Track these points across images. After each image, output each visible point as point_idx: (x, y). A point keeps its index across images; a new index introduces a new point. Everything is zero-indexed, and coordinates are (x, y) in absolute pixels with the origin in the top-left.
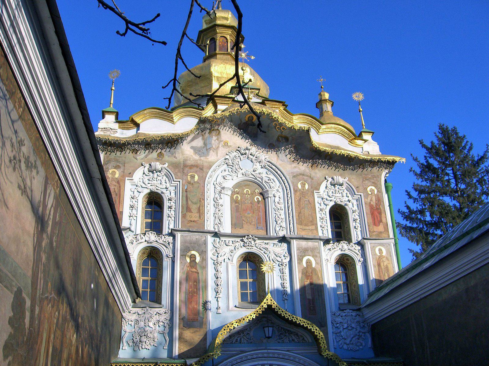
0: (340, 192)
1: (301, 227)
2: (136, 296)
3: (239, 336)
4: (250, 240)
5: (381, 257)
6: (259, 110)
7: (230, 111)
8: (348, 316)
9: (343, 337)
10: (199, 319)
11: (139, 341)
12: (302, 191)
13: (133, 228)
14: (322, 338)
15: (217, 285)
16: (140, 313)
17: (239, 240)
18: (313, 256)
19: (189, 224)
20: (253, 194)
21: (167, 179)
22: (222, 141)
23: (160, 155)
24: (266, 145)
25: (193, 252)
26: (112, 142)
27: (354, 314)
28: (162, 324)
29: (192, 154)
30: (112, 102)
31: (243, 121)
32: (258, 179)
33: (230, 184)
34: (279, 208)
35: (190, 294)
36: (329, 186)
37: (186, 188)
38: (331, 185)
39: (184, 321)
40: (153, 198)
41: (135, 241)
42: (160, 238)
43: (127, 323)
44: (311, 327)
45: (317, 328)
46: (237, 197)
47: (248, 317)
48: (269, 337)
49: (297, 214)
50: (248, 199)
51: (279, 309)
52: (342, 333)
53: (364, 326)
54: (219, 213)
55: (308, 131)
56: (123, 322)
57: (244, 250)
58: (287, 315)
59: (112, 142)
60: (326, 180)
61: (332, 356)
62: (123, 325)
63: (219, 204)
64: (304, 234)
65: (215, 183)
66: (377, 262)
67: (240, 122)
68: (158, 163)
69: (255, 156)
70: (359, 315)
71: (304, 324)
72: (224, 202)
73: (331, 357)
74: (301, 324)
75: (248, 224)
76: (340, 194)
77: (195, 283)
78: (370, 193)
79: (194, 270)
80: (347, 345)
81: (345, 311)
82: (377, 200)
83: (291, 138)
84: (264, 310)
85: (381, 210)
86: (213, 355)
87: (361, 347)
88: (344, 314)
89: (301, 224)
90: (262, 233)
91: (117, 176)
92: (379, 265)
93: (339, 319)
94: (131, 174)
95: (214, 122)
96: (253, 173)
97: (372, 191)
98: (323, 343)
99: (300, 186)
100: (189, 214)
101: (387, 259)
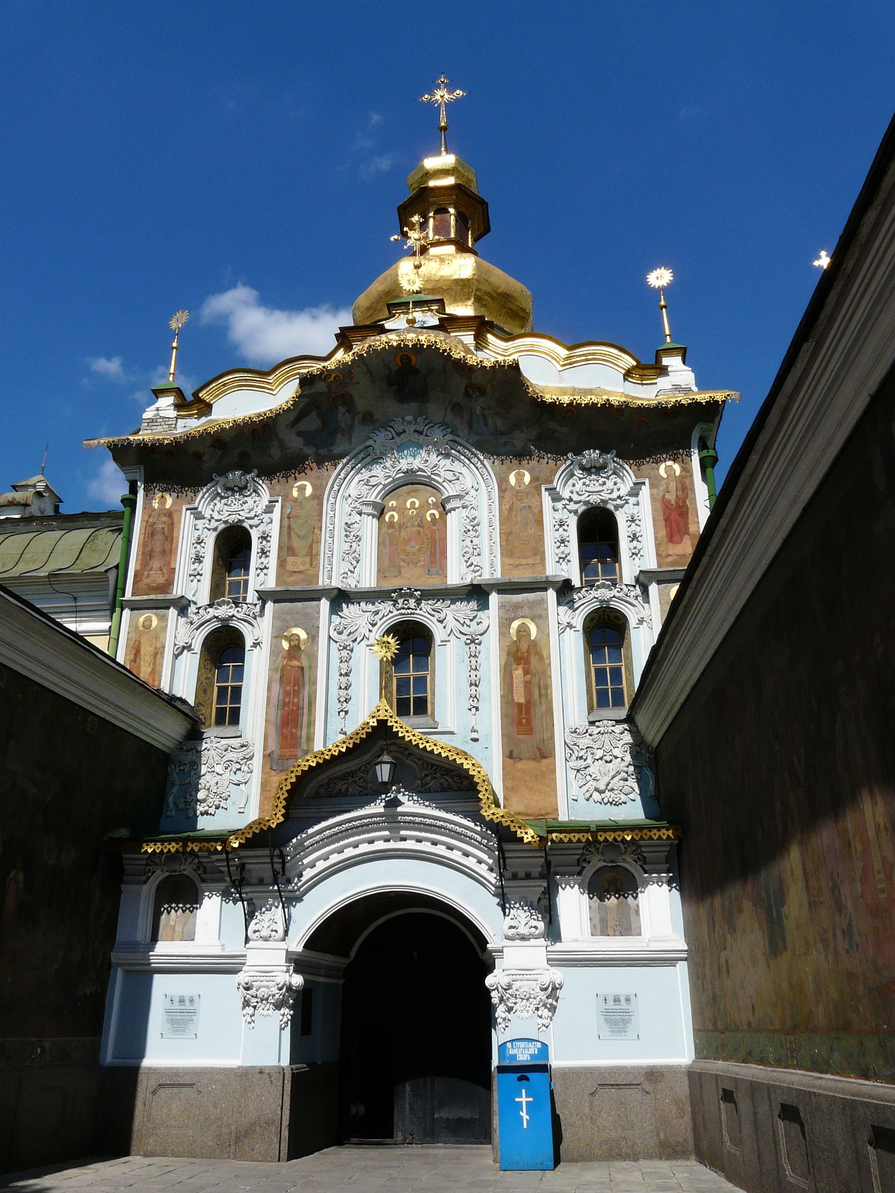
0: (600, 482)
12: (518, 488)
13: (194, 599)
14: (484, 781)
20: (425, 506)
21: (257, 499)
22: (359, 413)
23: (243, 456)
24: (447, 409)
27: (619, 728)
31: (394, 368)
34: (471, 528)
35: (286, 708)
37: (288, 511)
38: (583, 468)
42: (239, 609)
44: (463, 761)
46: (392, 516)
47: (337, 746)
49: (504, 538)
54: (351, 552)
55: (515, 368)
60: (568, 462)
61: (503, 816)
63: (352, 534)
69: (425, 433)
71: (449, 754)
74: (444, 755)
76: (600, 485)
77: (296, 688)
78: (665, 476)
79: (296, 663)
80: (601, 792)
81: (597, 724)
82: (680, 486)
86: (268, 821)
89: (512, 556)
90: (432, 583)
91: (167, 507)
95: (332, 379)
99: (512, 479)
100: (290, 559)
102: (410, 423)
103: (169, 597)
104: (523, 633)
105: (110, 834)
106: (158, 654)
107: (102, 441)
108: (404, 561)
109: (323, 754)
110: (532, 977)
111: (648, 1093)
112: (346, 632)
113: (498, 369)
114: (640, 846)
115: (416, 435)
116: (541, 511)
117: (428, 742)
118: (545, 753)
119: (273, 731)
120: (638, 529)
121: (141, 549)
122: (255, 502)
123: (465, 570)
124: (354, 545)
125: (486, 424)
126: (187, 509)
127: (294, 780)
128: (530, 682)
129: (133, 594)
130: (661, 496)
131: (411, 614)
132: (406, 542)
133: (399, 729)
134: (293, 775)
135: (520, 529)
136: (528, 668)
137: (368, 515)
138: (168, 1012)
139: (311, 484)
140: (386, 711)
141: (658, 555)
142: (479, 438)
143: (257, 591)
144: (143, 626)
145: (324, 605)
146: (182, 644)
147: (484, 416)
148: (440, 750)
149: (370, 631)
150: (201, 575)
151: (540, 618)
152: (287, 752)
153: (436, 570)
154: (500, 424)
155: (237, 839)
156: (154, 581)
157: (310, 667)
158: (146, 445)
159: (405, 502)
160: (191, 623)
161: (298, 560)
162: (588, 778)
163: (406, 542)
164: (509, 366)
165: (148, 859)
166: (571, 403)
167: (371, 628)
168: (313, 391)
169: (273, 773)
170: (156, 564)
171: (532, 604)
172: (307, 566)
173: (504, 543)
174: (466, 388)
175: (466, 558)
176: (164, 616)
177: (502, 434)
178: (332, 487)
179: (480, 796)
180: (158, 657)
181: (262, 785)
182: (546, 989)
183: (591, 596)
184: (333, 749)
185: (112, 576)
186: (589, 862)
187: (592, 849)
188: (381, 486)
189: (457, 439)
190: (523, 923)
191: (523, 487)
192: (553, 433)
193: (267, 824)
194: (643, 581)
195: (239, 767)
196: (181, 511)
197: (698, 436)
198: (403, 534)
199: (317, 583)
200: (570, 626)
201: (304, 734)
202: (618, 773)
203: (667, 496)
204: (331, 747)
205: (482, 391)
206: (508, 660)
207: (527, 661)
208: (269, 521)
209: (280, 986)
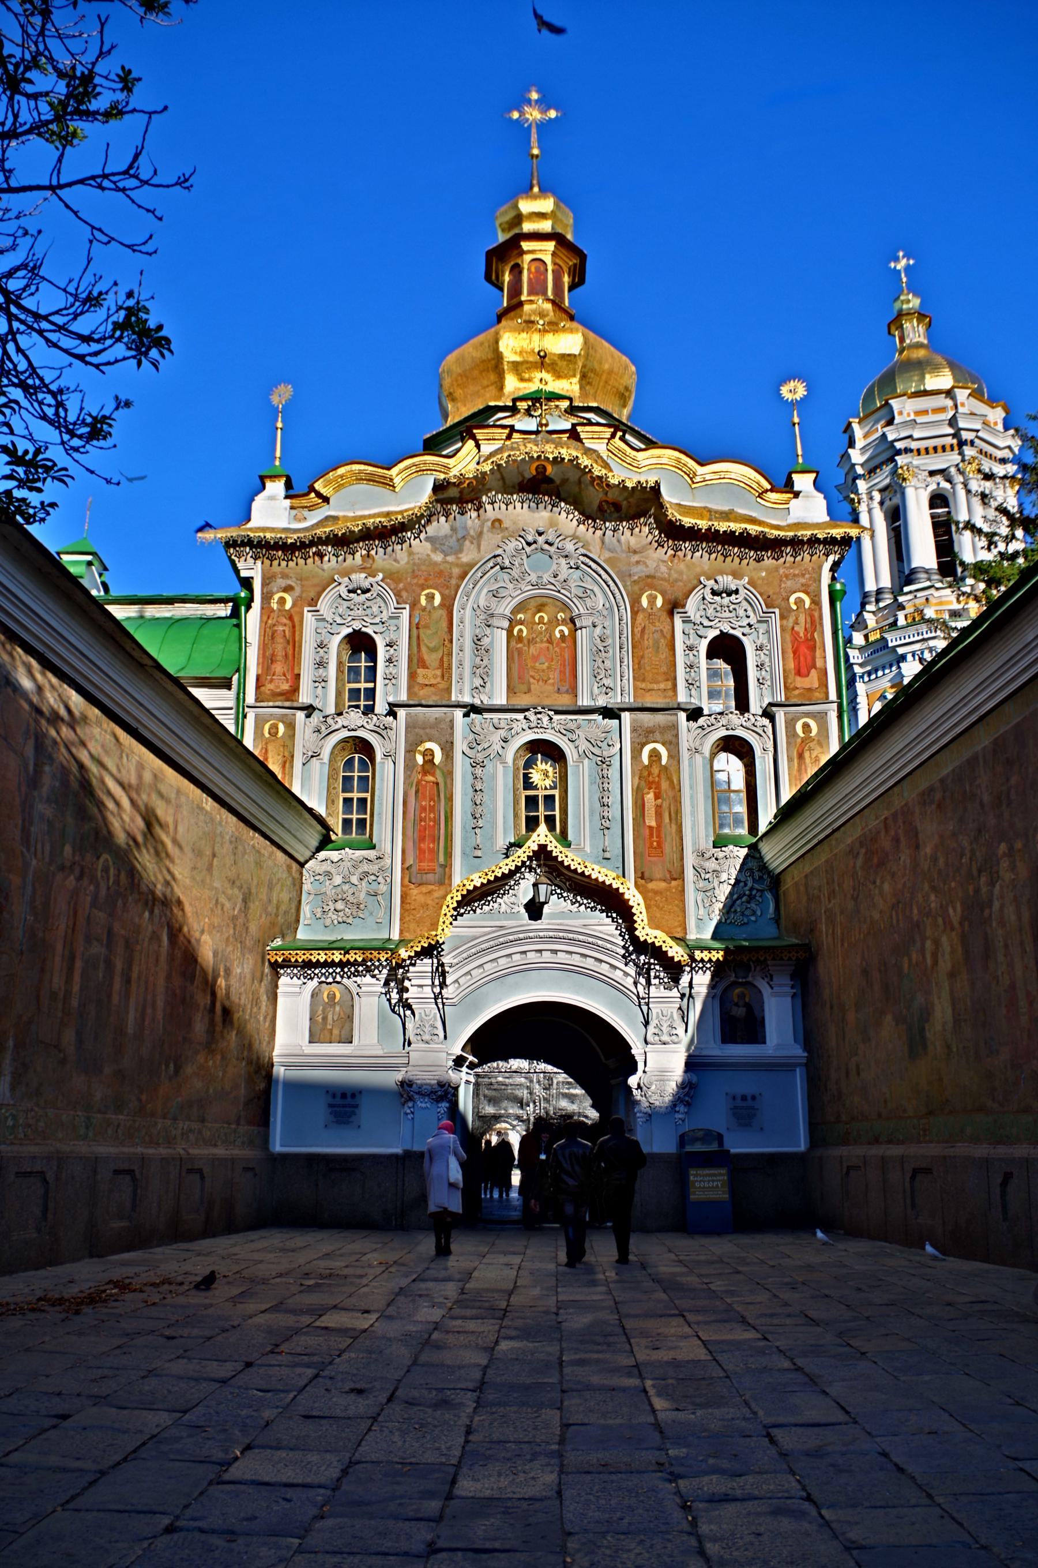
1: (643, 686)
2: (324, 832)
4: (539, 716)
5: (807, 739)
6: (552, 453)
17: (520, 716)
18: (663, 744)
19: (422, 693)
20: (554, 622)
21: (383, 605)
22: (488, 520)
25: (429, 745)
26: (272, 542)
30: (278, 454)
31: (528, 476)
32: (562, 591)
33: (506, 607)
36: (709, 597)
37: (417, 620)
41: (323, 728)
46: (521, 631)
49: (636, 661)
50: (541, 633)
53: (761, 878)
55: (656, 490)
58: (575, 863)
59: (272, 542)
65: (475, 606)
67: (520, 479)
68: (363, 575)
69: (556, 545)
72: (492, 642)
75: (540, 683)
77: (432, 803)
78: (794, 607)
79: (430, 778)
82: (809, 620)
83: (625, 503)
88: (721, 855)
89: (644, 680)
91: (288, 605)
94: (313, 602)
96: (552, 580)
97: (799, 602)
99: (644, 602)
103: (295, 705)
104: (654, 758)
106: (288, 761)
107: (219, 536)
112: (480, 748)
115: (546, 547)
119: (410, 845)
123: (596, 691)
128: (661, 806)
129: (257, 700)
132: (535, 658)
136: (659, 793)
138: (330, 1106)
139: (440, 593)
142: (611, 555)
143: (389, 704)
146: (310, 754)
151: (673, 746)
152: (425, 865)
153: (564, 689)
156: (278, 687)
161: (429, 673)
163: (535, 658)
164: (651, 488)
167: (504, 744)
169: (412, 886)
170: (279, 668)
172: (439, 680)
173: (636, 666)
174: (601, 502)
177: (635, 552)
180: (287, 765)
181: (402, 896)
185: (235, 678)
198: (532, 650)
200: (697, 751)
204: (494, 868)
207: (658, 786)
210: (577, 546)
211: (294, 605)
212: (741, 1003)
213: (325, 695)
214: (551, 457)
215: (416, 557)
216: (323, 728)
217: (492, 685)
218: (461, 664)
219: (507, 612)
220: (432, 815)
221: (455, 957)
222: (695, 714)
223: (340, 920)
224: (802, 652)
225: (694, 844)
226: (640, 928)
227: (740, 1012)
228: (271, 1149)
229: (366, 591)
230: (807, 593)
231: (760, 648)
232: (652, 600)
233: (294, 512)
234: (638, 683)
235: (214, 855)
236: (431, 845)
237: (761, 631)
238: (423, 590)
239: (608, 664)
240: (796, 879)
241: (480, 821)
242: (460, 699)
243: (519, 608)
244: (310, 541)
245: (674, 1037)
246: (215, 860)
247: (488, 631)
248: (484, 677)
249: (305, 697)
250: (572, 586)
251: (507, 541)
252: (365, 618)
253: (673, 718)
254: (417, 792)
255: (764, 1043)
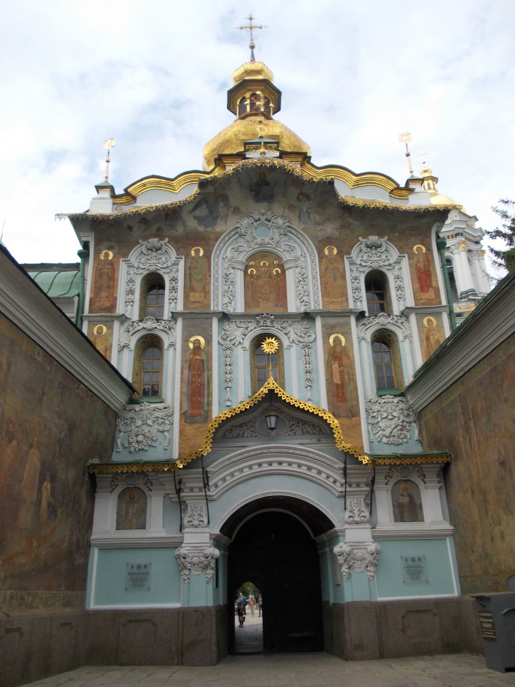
0: (378, 255)
1: (328, 300)
2: (131, 391)
3: (242, 429)
6: (269, 163)
7: (233, 169)
8: (387, 403)
9: (382, 428)
10: (202, 412)
11: (135, 442)
12: (330, 257)
14: (337, 427)
15: (226, 373)
16: (137, 410)
19: (192, 306)
21: (167, 256)
22: (231, 207)
23: (159, 229)
24: (285, 208)
27: (396, 400)
28: (163, 421)
29: (196, 226)
31: (255, 181)
32: (277, 248)
33: (242, 257)
35: (194, 385)
37: (189, 265)
38: (367, 246)
39: (186, 417)
40: (156, 280)
43: (123, 422)
44: (323, 415)
45: (330, 415)
46: (252, 271)
47: (244, 405)
48: (272, 429)
49: (323, 286)
50: (265, 272)
51: (283, 394)
52: (380, 424)
53: (408, 414)
54: (229, 292)
55: (331, 183)
56: (117, 421)
57: (258, 331)
58: (293, 401)
61: (349, 448)
62: (118, 424)
63: (229, 280)
64: (332, 308)
65: (224, 257)
66: (426, 336)
68: (156, 239)
69: (272, 221)
70: (402, 401)
71: (314, 410)
73: (348, 450)
74: (311, 411)
77: (199, 373)
78: (417, 253)
79: (198, 357)
80: (388, 437)
81: (383, 397)
84: (264, 396)
85: (431, 272)
86: (202, 451)
87: (405, 440)
88: (383, 401)
89: (328, 297)
92: (428, 339)
93: (376, 407)
94: (126, 255)
95: (218, 184)
96: (270, 242)
98: (338, 432)
99: (326, 252)
100: (192, 294)
101: (438, 331)
102: (263, 215)
103: (114, 314)
105: (90, 461)
106: (109, 348)
108: (261, 298)
109: (235, 410)
110: (364, 547)
111: (435, 615)
112: (229, 339)
113: (322, 183)
114: (422, 468)
115: (267, 222)
116: (344, 271)
117: (300, 403)
118: (354, 413)
119: (185, 398)
120: (401, 284)
121: (93, 284)
122: (166, 258)
123: (299, 304)
124: (231, 287)
125: (309, 218)
126: (123, 261)
127: (217, 426)
129: (89, 313)
130: (414, 265)
131: (269, 329)
133: (282, 395)
134: (216, 423)
135: (332, 281)
137: (238, 269)
138: (130, 574)
140: (273, 384)
141: (415, 299)
143: (172, 313)
144: (97, 332)
145: (215, 322)
146: (122, 344)
147: (309, 213)
148: (308, 408)
149: (243, 339)
150: (133, 302)
151: (348, 334)
152: (196, 412)
154: (318, 218)
155: (181, 463)
157: (208, 360)
158: (98, 218)
159: (260, 262)
160: (128, 332)
161: (197, 295)
162: (379, 429)
164: (329, 182)
165: (113, 477)
166: (364, 207)
167: (243, 337)
168: (205, 191)
169: (187, 425)
170: (104, 294)
171: (342, 325)
172: (203, 298)
173: (323, 289)
175: (300, 297)
176: (111, 326)
177: (319, 224)
178: (216, 252)
179: (335, 436)
180: (108, 352)
182: (372, 554)
183: (376, 322)
184: (242, 407)
186: (392, 477)
187: (394, 470)
188: (245, 253)
189: (292, 225)
190: (357, 514)
191: (333, 256)
192: (350, 225)
193: (201, 453)
194: (405, 314)
195: (163, 421)
196: (119, 262)
197: (435, 230)
198: (260, 282)
199: (210, 308)
201: (206, 401)
202: (396, 427)
203: (419, 265)
204: (240, 406)
205: (308, 197)
206: (328, 359)
207: (340, 359)
208: (176, 270)
209: (207, 556)
210: (284, 221)
211: (114, 257)
212: (405, 494)
213: (132, 311)
214: (268, 165)
215: (189, 228)
216: (131, 328)
217: (235, 302)
218: (216, 289)
219: (244, 260)
220: (199, 380)
221: (214, 467)
222: (360, 316)
223: (140, 447)
224: (423, 278)
225: (365, 394)
226: (339, 443)
227: (405, 500)
228: (87, 607)
229: (157, 250)
230: (423, 245)
231: (398, 277)
232: (331, 251)
233: (115, 206)
234: (325, 298)
235: (44, 394)
236: (199, 399)
237: (397, 267)
238: (193, 247)
239: (305, 287)
240: (434, 412)
241: (230, 383)
242: (216, 308)
243: (251, 258)
244: (124, 218)
245: (363, 518)
246: (45, 397)
247: (232, 271)
248: (231, 297)
249: (120, 310)
250: (283, 245)
251: (243, 219)
252: (157, 265)
253: (347, 318)
254: (189, 366)
255: (423, 521)
